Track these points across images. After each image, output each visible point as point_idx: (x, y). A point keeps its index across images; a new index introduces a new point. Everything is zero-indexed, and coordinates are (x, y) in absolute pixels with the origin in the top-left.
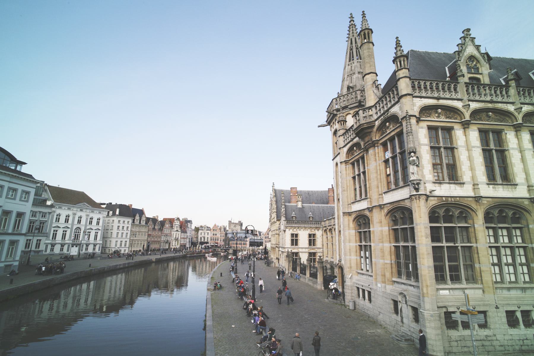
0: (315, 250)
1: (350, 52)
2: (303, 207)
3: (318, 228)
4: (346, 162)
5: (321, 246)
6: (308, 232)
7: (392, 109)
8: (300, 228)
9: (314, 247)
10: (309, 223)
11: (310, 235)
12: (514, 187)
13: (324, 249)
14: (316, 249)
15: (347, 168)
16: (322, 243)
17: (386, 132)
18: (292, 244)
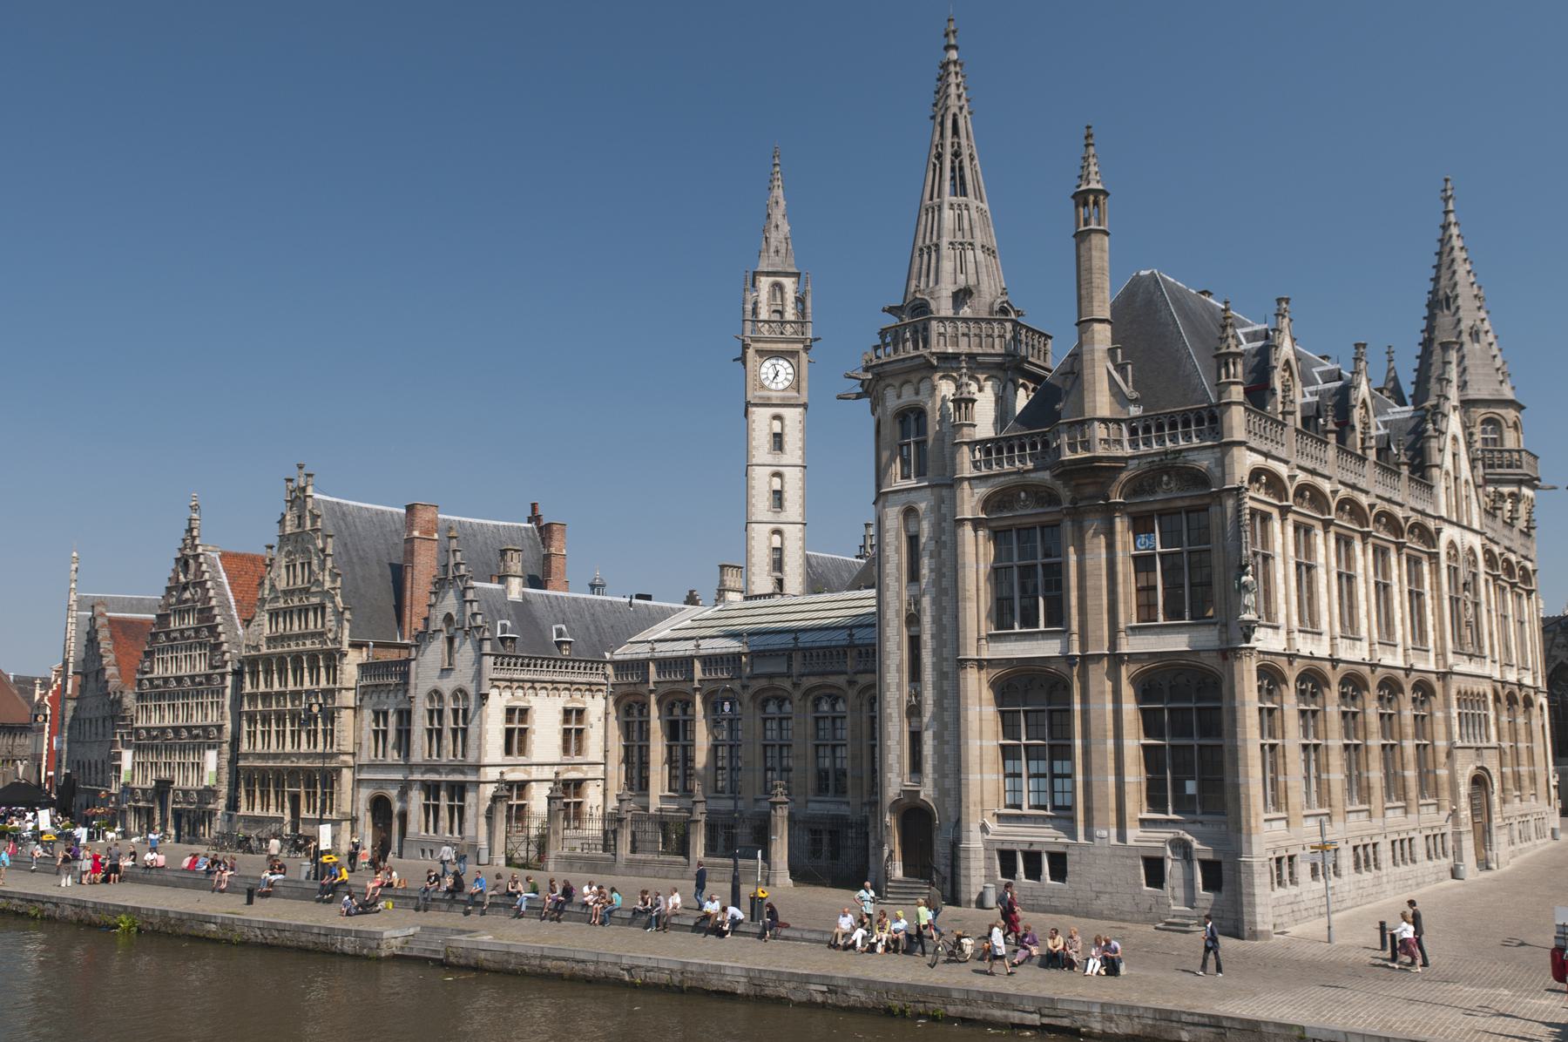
0: (582, 771)
1: (953, 162)
2: (526, 600)
3: (591, 688)
4: (977, 524)
5: (599, 758)
6: (561, 701)
7: (1190, 453)
8: (537, 685)
9: (578, 759)
10: (535, 666)
11: (567, 712)
12: (1316, 637)
13: (609, 768)
14: (584, 767)
15: (981, 539)
16: (602, 744)
17: (1153, 492)
18: (508, 751)
